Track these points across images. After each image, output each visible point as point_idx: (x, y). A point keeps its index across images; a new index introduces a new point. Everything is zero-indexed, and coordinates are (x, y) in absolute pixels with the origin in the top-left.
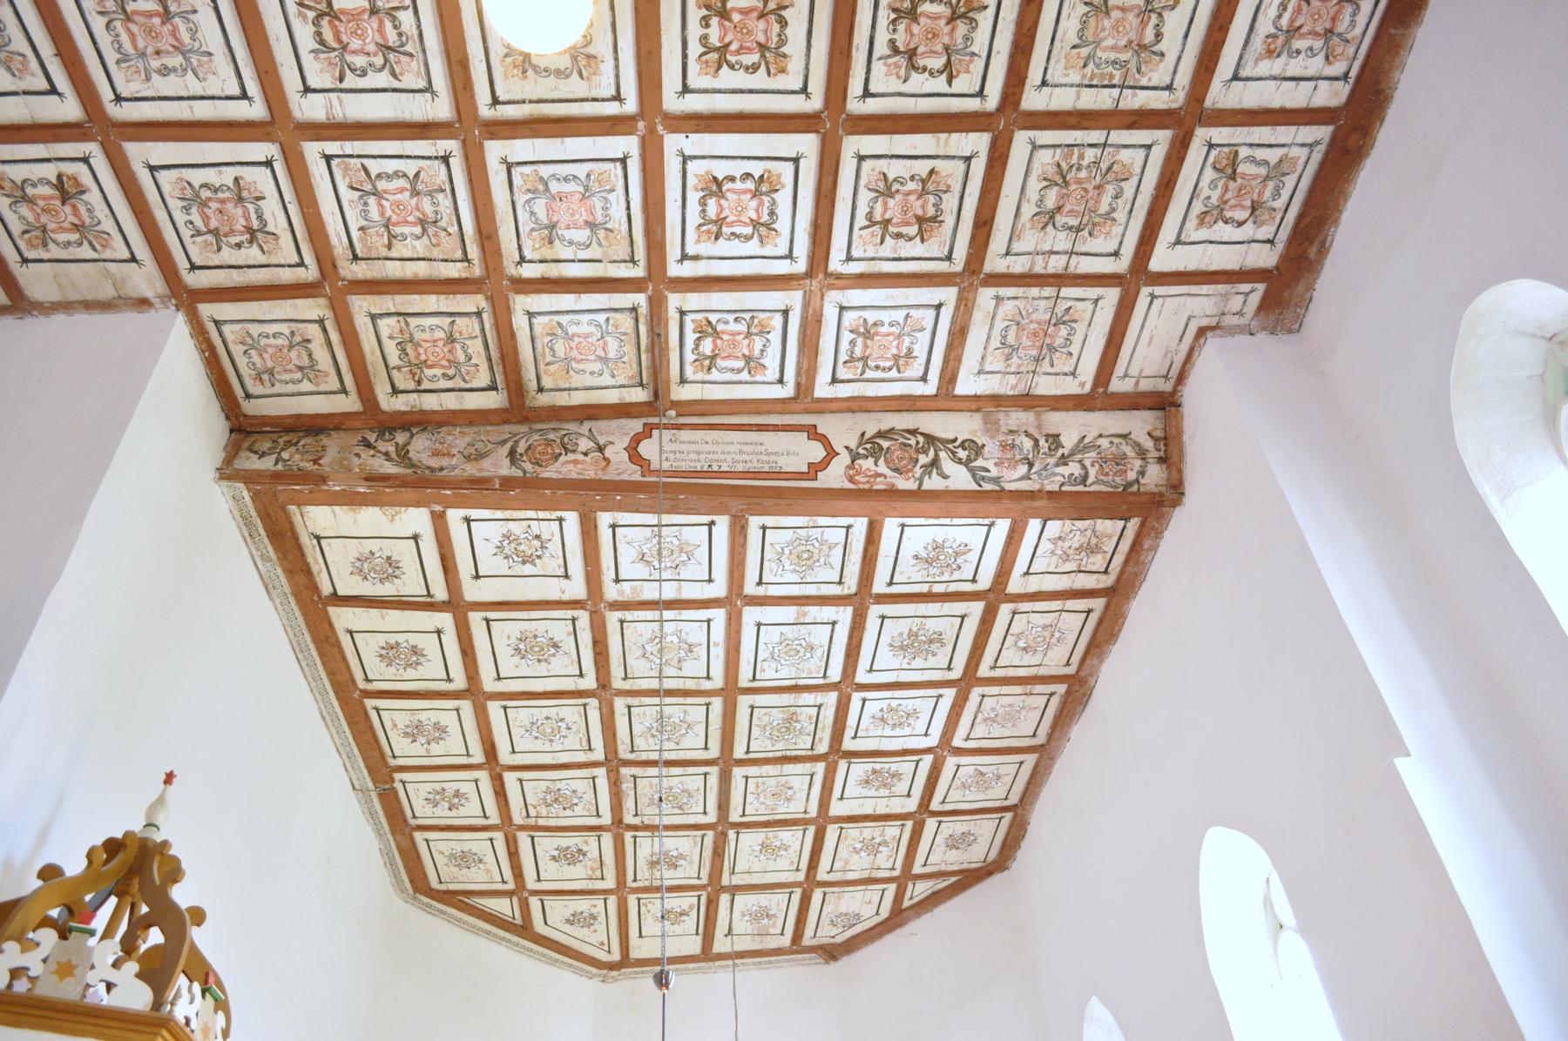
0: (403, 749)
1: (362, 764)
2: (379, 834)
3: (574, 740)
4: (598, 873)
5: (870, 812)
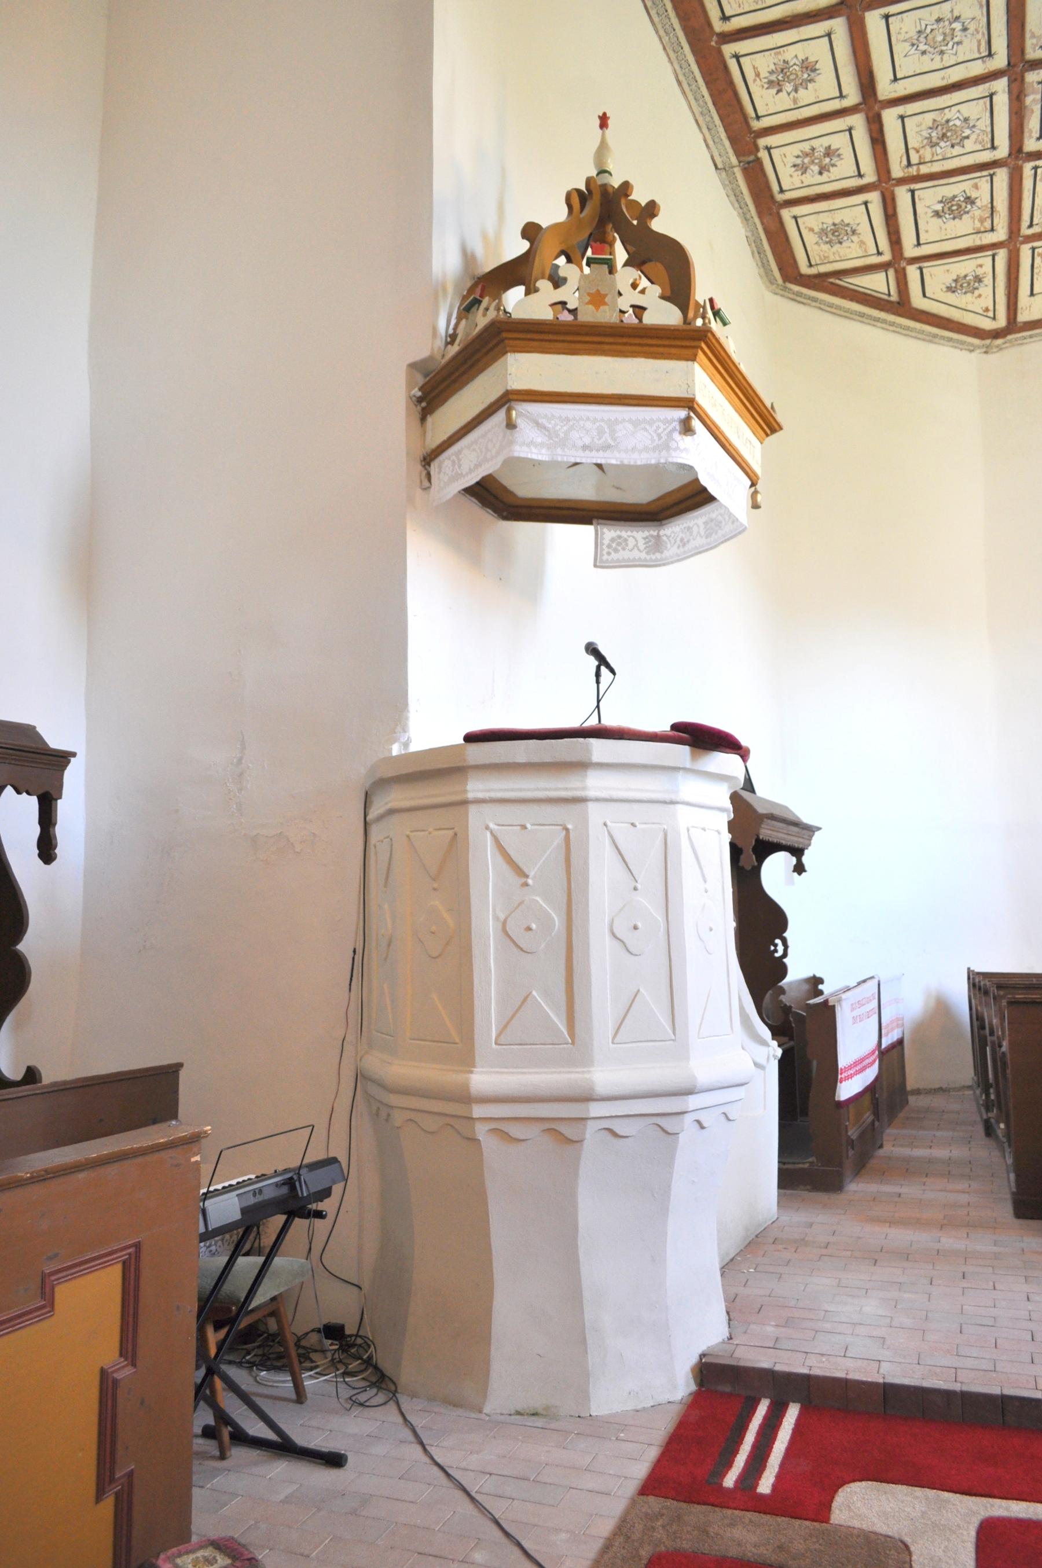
0: (768, 104)
1: (723, 135)
2: (746, 219)
3: (970, 47)
4: (988, 225)
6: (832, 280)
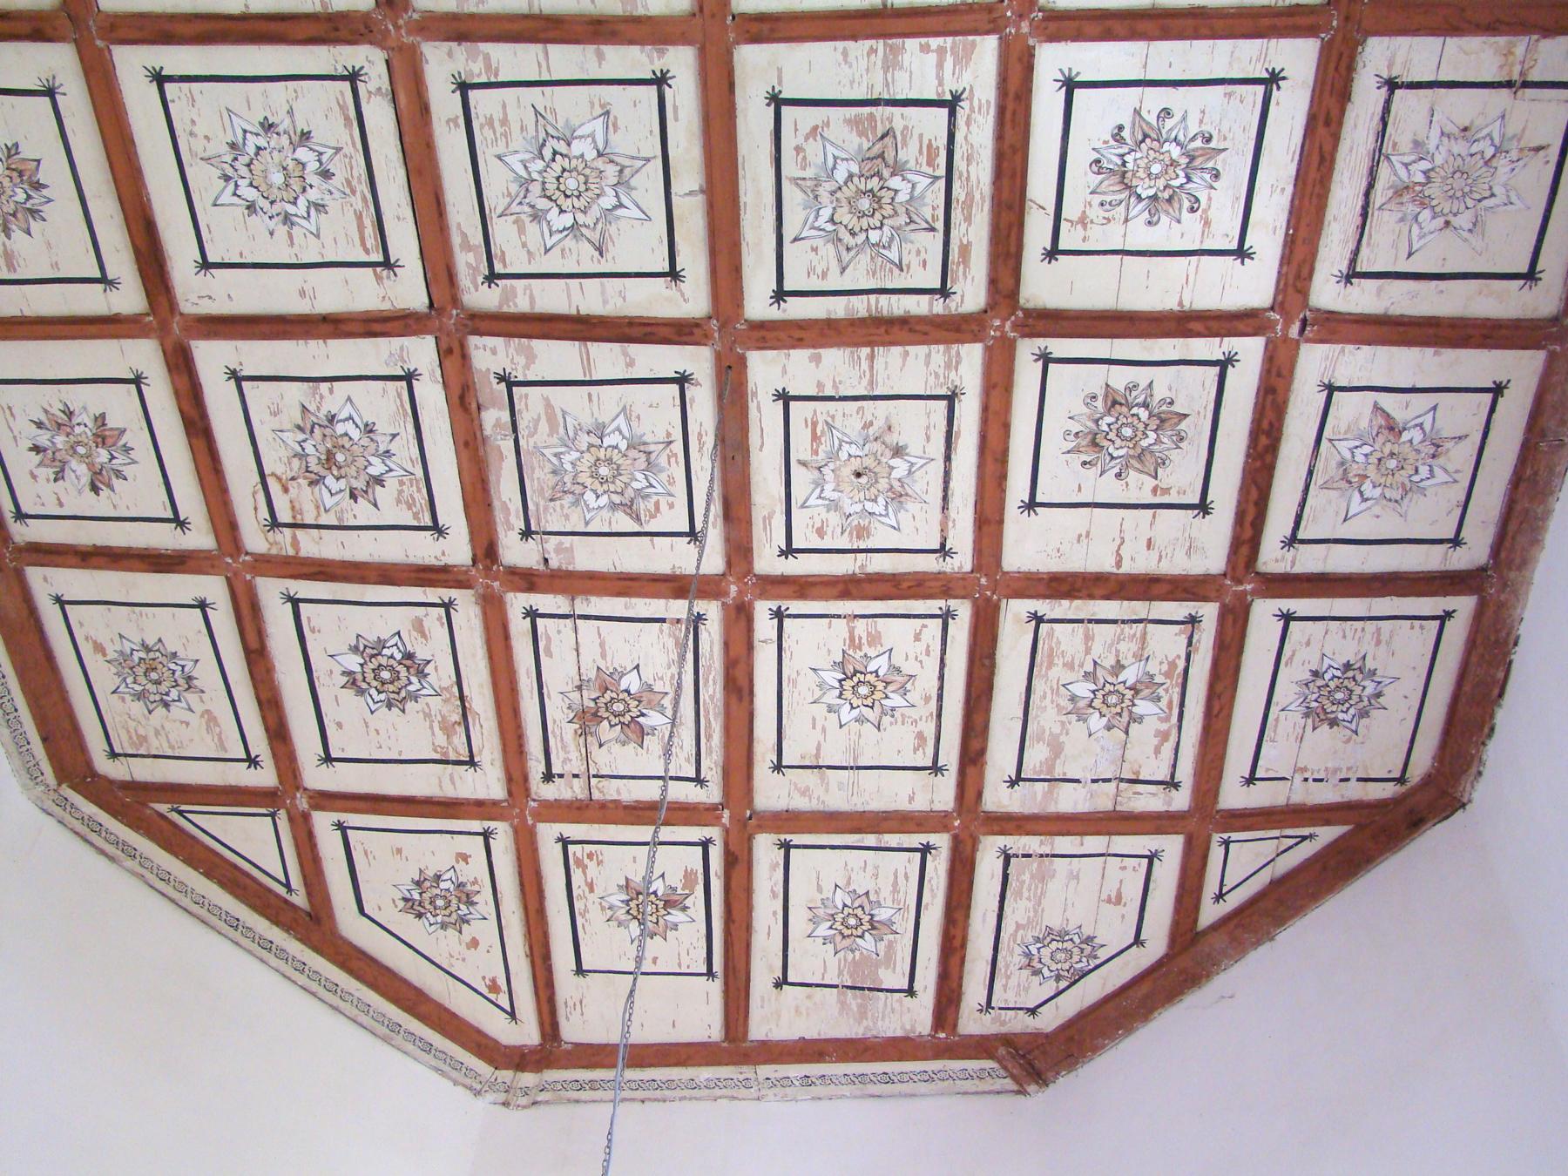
5: (1106, 565)
6: (163, 808)
